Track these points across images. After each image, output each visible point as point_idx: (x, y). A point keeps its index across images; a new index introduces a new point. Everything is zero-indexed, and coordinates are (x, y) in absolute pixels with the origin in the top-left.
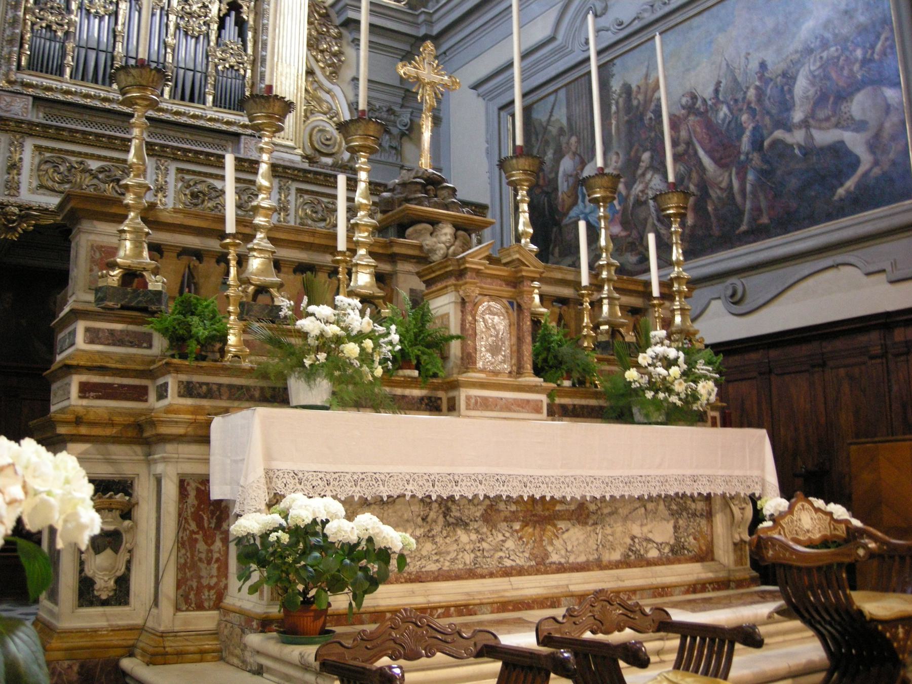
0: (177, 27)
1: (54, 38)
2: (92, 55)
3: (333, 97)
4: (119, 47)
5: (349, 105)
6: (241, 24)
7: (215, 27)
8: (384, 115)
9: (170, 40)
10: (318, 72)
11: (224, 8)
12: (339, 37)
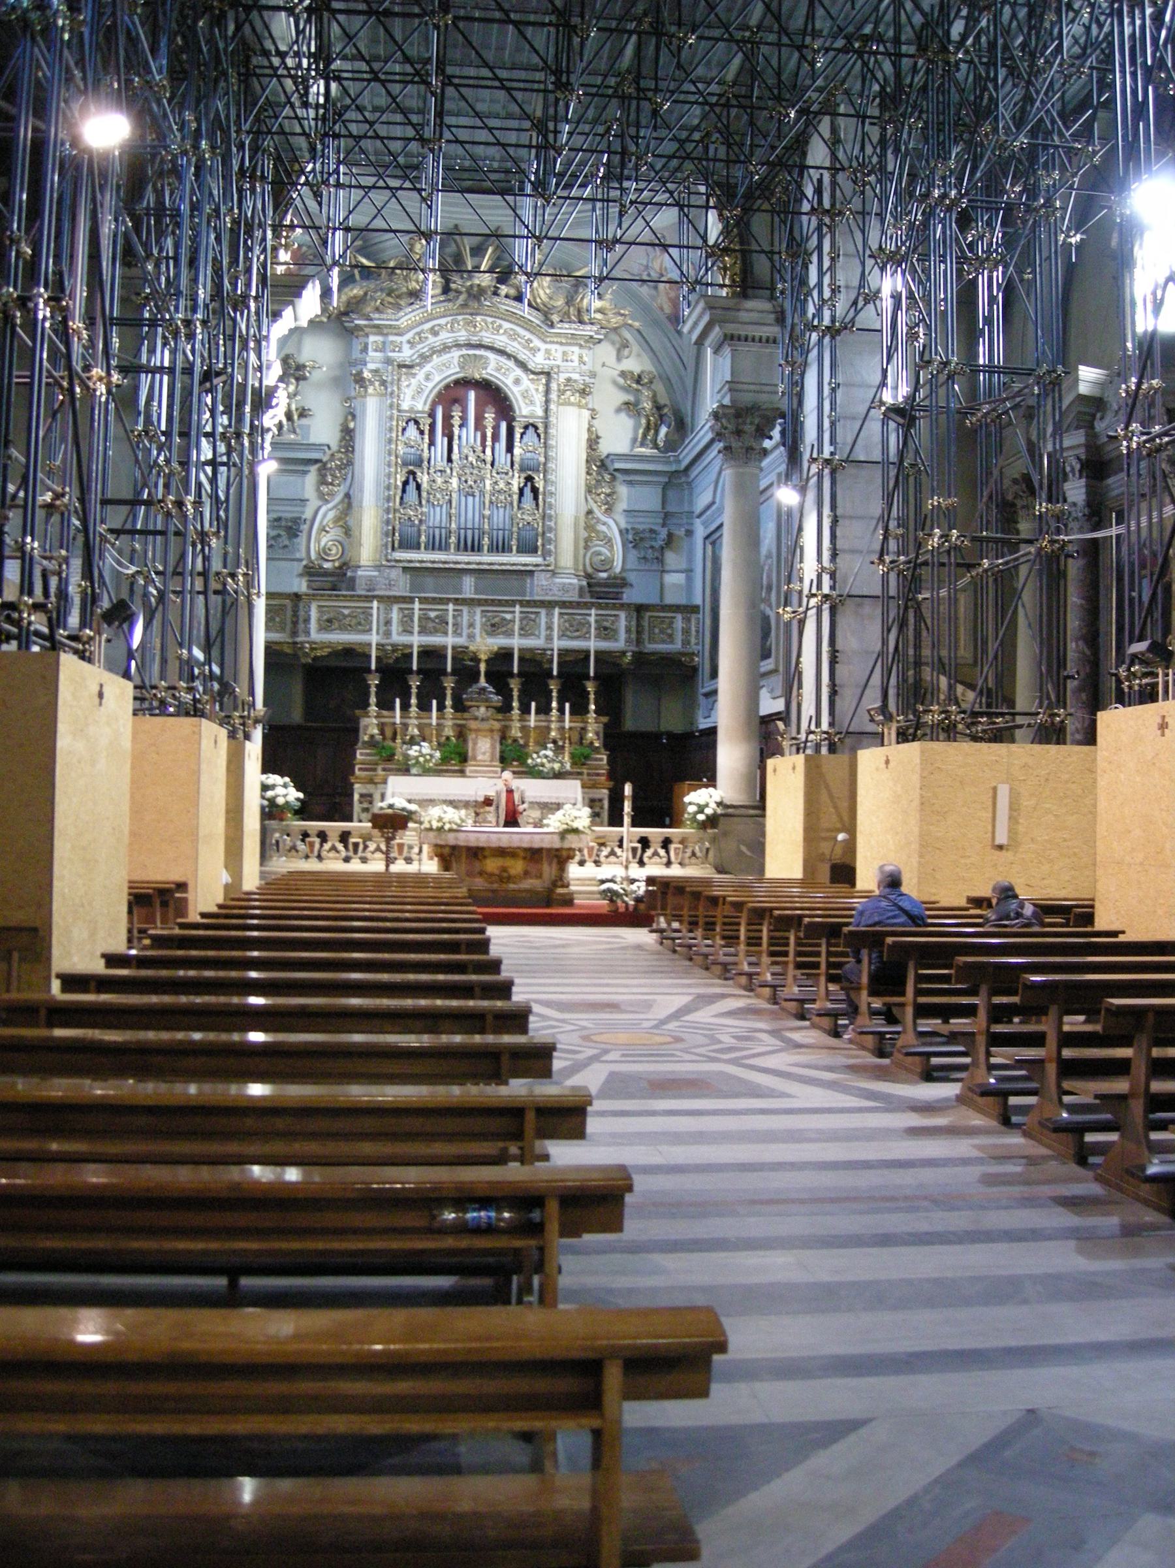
0: (491, 502)
1: (413, 525)
2: (437, 532)
3: (609, 527)
4: (453, 526)
5: (621, 531)
6: (535, 491)
7: (516, 497)
8: (647, 535)
9: (487, 512)
10: (596, 510)
11: (522, 480)
12: (614, 478)
